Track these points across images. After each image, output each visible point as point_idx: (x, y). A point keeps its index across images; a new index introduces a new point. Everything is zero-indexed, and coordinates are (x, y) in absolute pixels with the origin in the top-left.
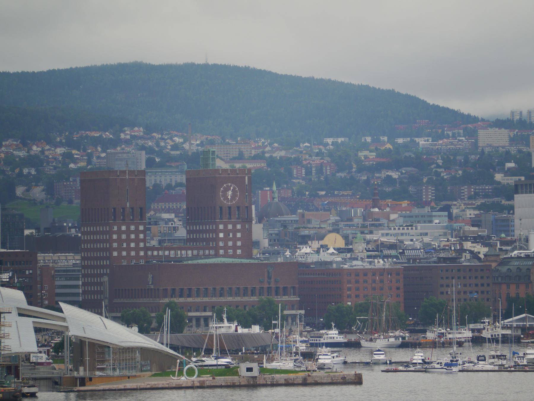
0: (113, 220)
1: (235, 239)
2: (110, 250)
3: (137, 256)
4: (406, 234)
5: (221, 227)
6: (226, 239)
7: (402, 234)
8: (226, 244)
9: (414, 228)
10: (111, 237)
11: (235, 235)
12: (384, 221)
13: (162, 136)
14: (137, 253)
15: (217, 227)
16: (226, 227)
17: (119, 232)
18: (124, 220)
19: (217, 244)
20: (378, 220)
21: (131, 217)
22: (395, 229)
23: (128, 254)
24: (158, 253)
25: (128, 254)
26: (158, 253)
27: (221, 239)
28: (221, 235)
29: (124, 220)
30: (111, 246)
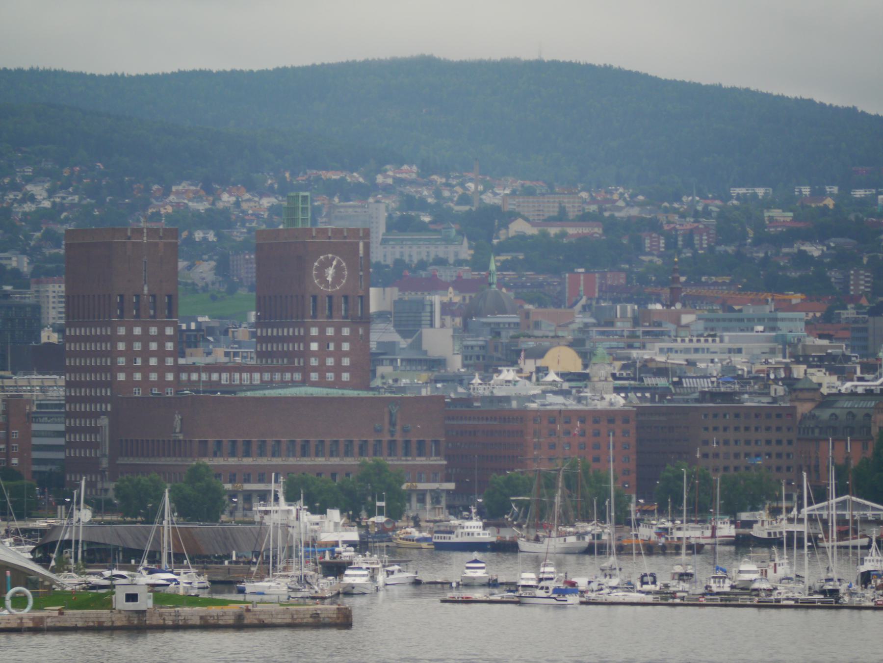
0: (118, 317)
1: (339, 354)
2: (113, 369)
3: (162, 383)
4: (703, 349)
5: (314, 331)
6: (322, 353)
7: (696, 350)
8: (322, 363)
9: (718, 339)
10: (114, 346)
11: (338, 347)
12: (670, 327)
13: (447, 180)
14: (162, 377)
15: (307, 331)
16: (322, 331)
17: (130, 339)
18: (138, 316)
19: (307, 362)
20: (659, 325)
21: (152, 312)
22: (691, 341)
23: (146, 377)
24: (200, 376)
25: (146, 377)
26: (200, 376)
27: (314, 354)
28: (314, 346)
29: (138, 316)
30: (114, 362)
